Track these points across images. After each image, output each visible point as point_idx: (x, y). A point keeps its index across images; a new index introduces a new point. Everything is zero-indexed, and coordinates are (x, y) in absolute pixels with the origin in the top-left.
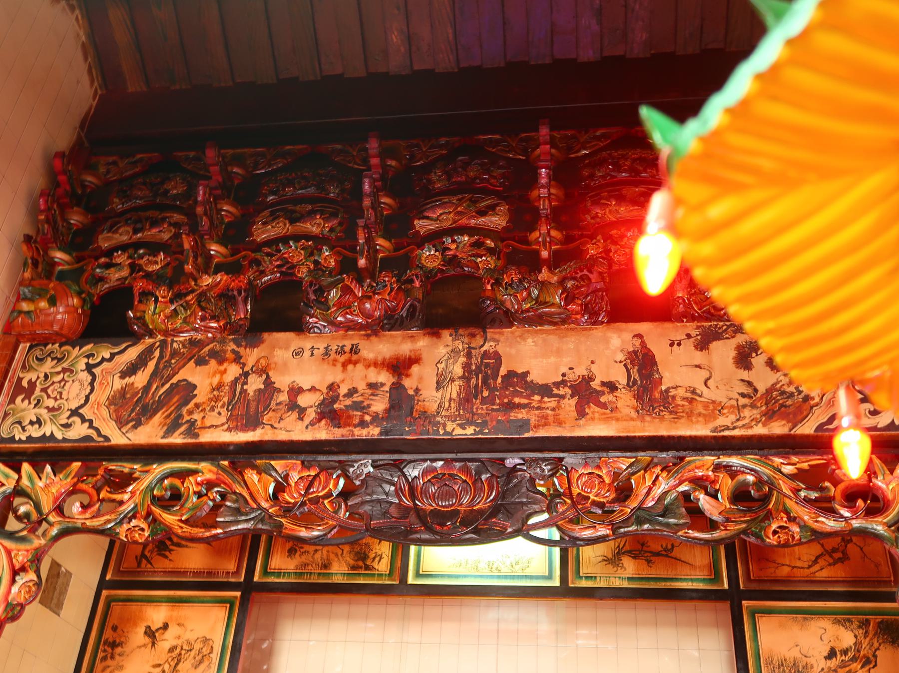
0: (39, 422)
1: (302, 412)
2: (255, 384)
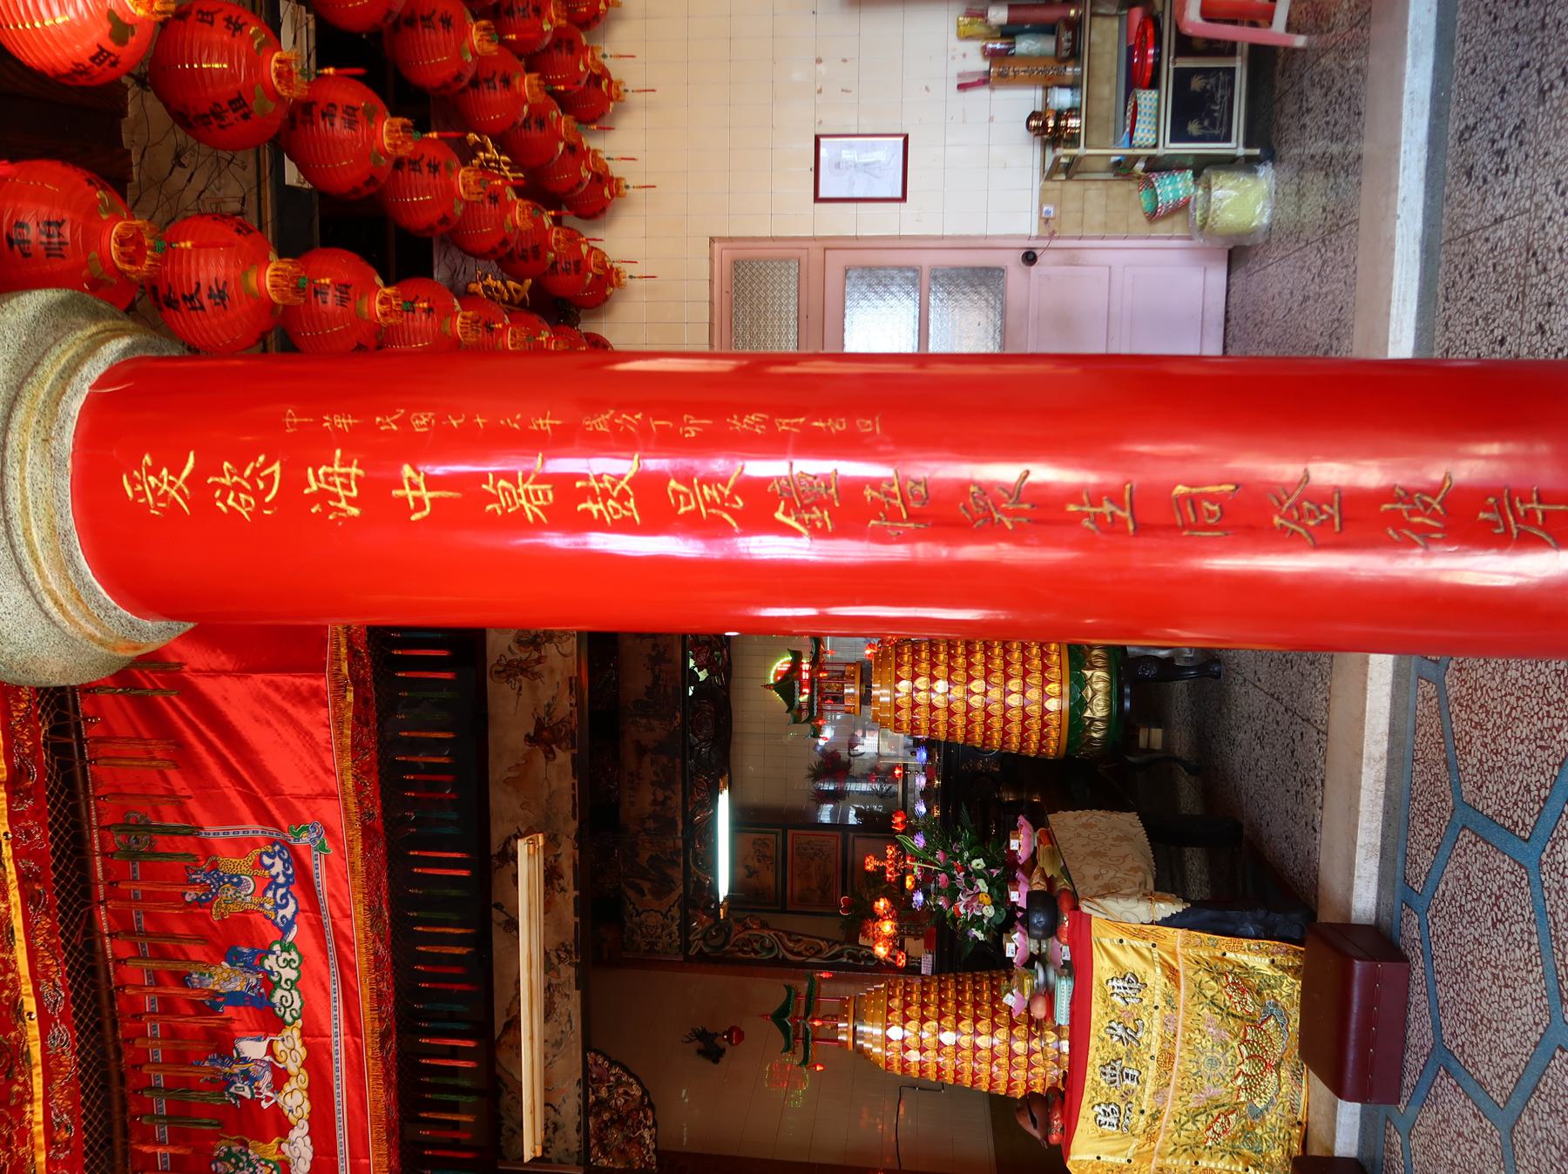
0: (670, 935)
1: (667, 798)
2: (650, 824)
